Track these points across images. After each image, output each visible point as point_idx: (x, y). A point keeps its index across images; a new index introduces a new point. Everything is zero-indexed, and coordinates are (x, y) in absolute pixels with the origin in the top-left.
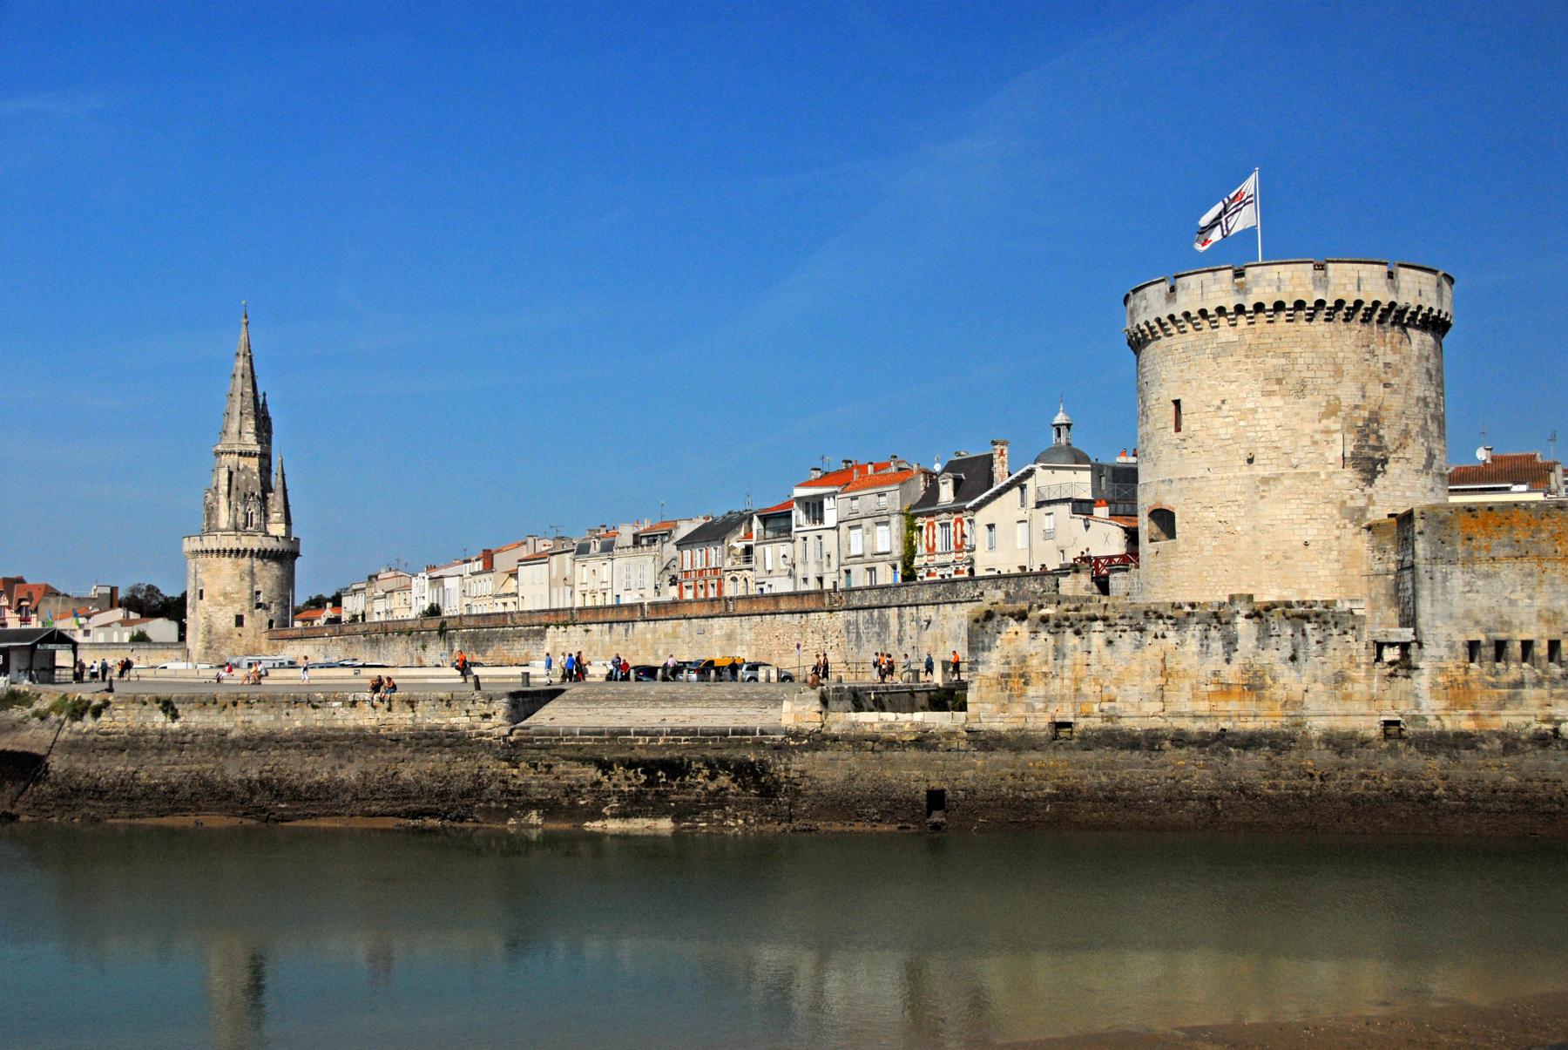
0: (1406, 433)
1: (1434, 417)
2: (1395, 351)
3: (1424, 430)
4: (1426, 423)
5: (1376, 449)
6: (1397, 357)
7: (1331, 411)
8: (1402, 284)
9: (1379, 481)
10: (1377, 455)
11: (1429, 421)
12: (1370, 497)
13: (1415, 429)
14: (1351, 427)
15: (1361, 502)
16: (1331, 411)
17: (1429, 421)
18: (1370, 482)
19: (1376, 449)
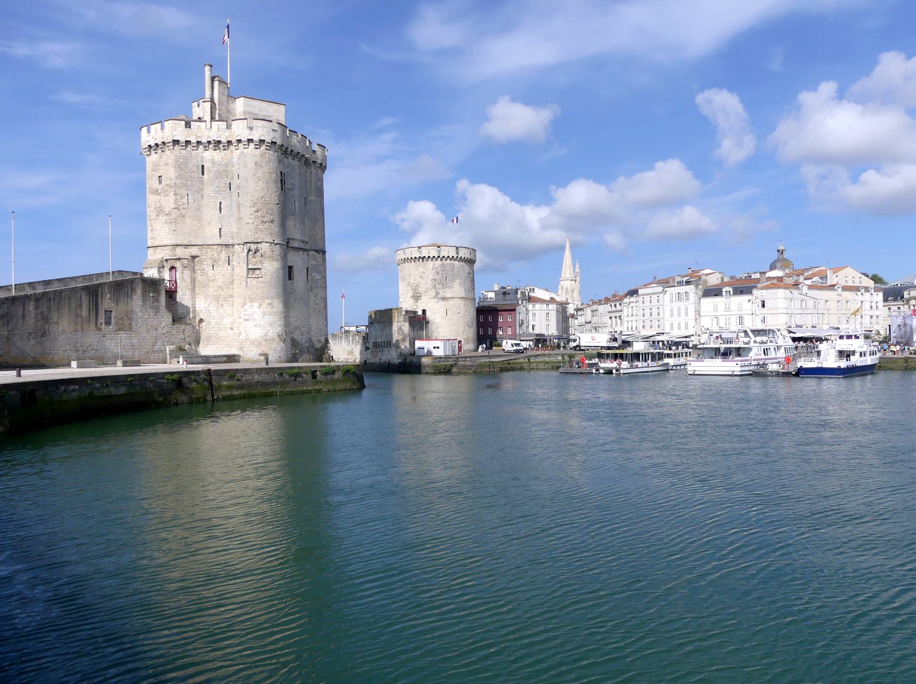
0: (427, 289)
1: (439, 284)
2: (424, 268)
3: (434, 287)
4: (435, 285)
5: (417, 293)
6: (424, 270)
7: (408, 285)
8: (422, 251)
9: (419, 301)
10: (419, 295)
11: (437, 285)
12: (417, 306)
13: (430, 288)
14: (412, 289)
15: (415, 307)
16: (408, 285)
17: (437, 285)
18: (417, 302)
19: (417, 293)
